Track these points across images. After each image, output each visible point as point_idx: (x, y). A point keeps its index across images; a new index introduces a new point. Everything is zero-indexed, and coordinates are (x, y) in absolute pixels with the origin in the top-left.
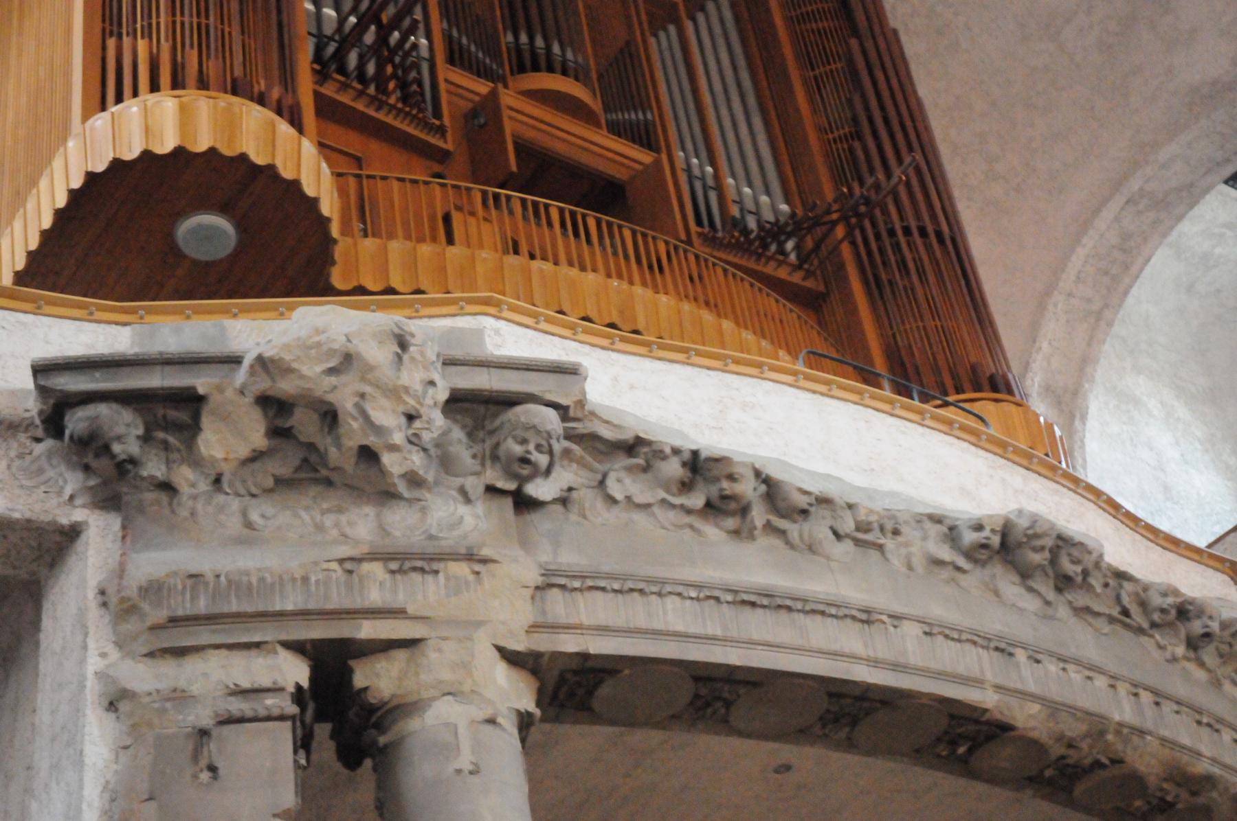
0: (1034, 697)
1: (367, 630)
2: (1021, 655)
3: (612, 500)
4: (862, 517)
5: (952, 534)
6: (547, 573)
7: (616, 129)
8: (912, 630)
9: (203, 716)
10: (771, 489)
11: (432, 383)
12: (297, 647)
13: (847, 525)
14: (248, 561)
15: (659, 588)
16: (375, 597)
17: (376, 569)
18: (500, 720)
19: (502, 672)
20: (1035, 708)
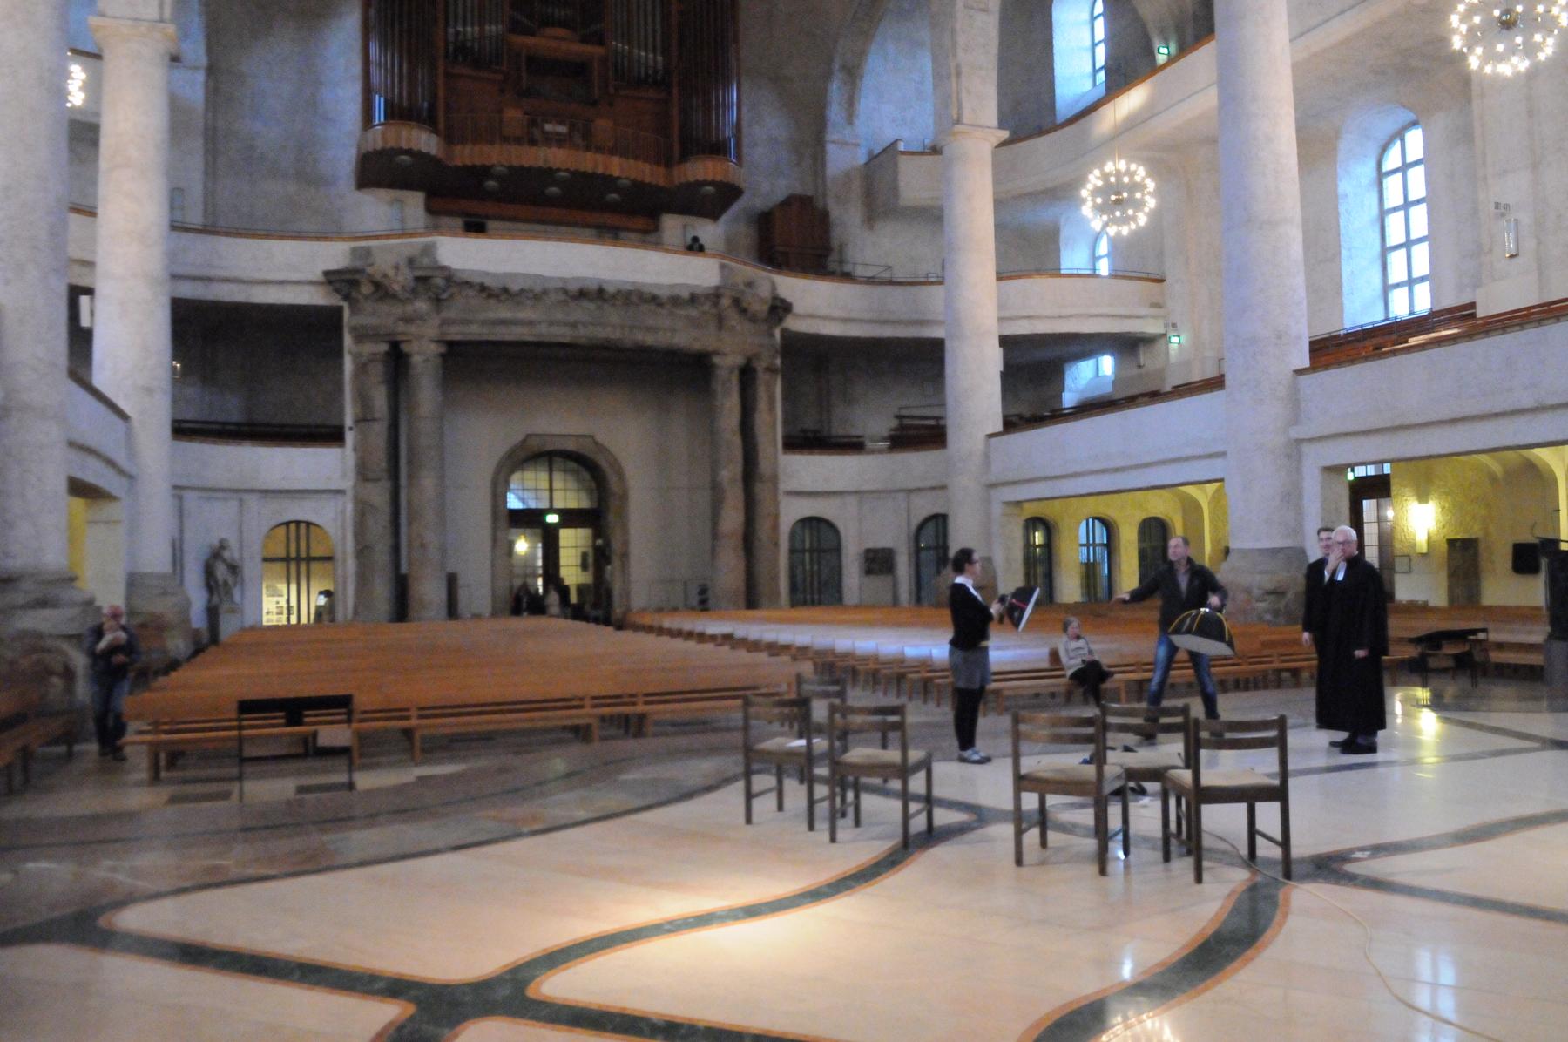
1: (399, 338)
5: (565, 291)
7: (584, 40)
9: (364, 359)
10: (505, 290)
12: (386, 342)
13: (531, 295)
14: (374, 321)
15: (468, 322)
17: (401, 323)
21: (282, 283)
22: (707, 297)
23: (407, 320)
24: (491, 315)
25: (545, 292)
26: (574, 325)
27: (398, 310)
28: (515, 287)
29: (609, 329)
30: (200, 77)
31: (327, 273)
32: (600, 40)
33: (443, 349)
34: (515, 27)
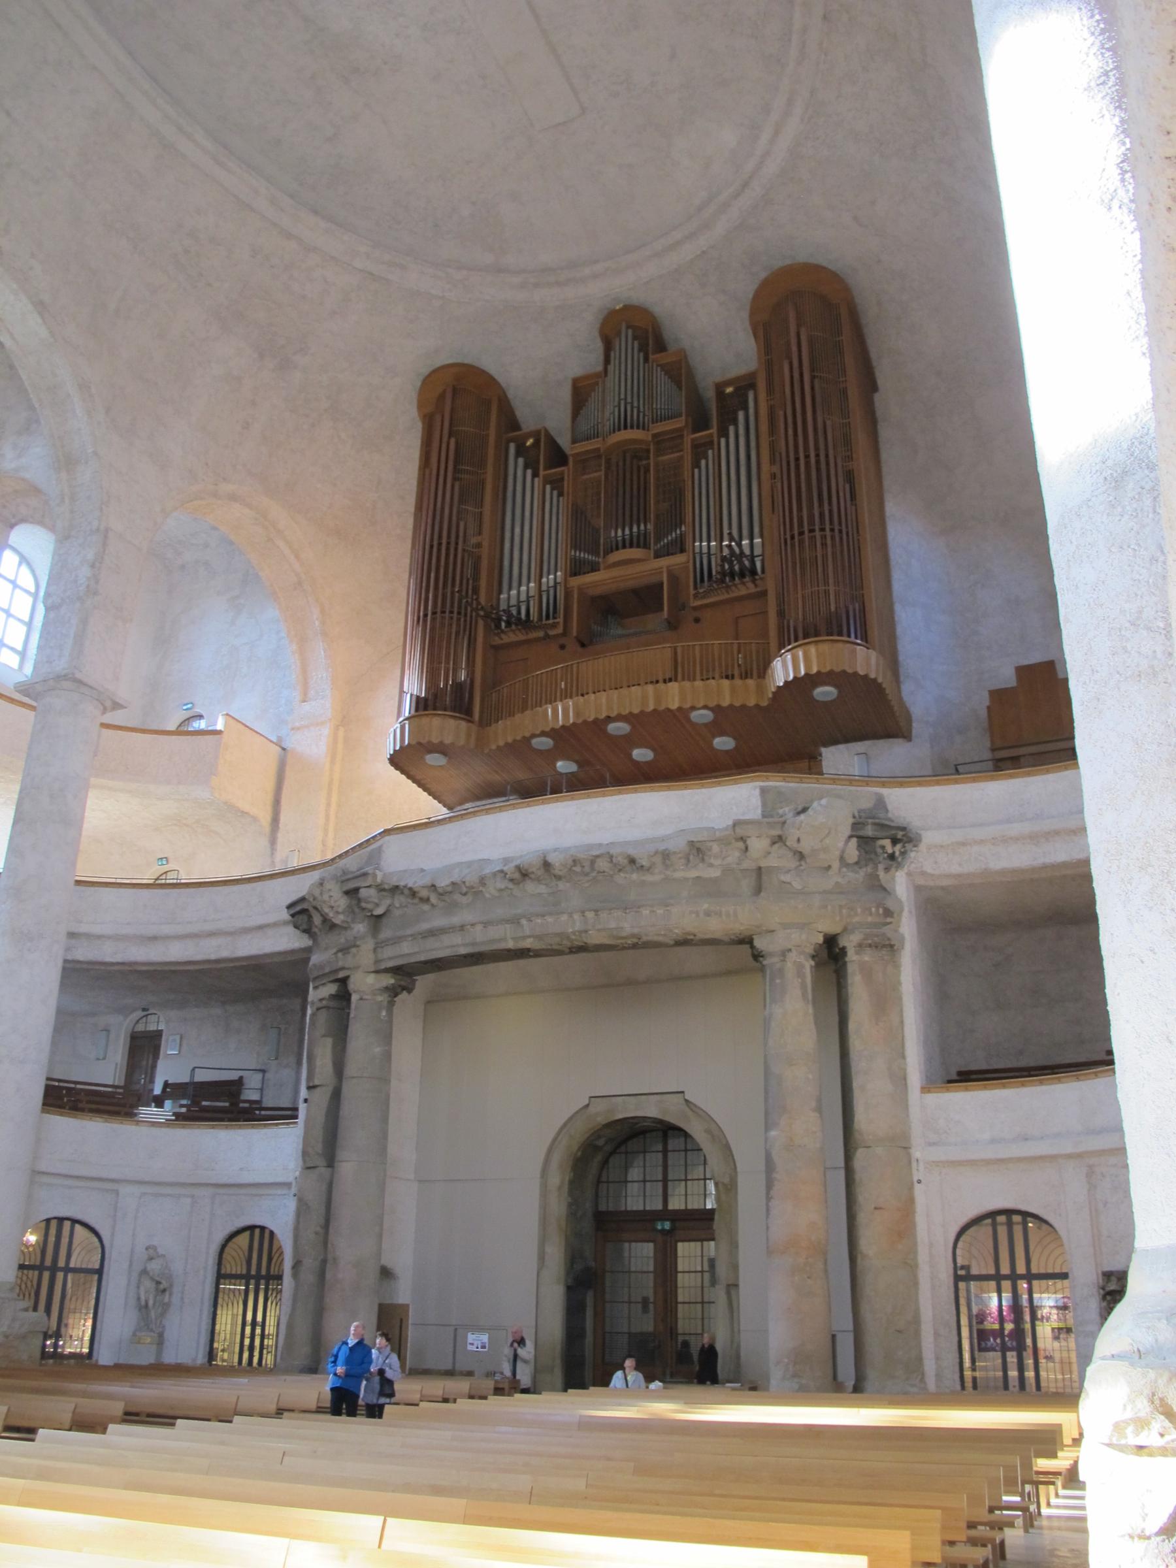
0: (529, 937)
1: (341, 975)
2: (524, 922)
3: (397, 908)
4: (467, 884)
6: (377, 943)
8: (479, 927)
11: (331, 896)
16: (340, 964)
17: (340, 955)
18: (365, 997)
19: (371, 979)
20: (531, 940)
21: (261, 928)
22: (723, 841)
23: (345, 950)
24: (425, 926)
25: (482, 881)
26: (515, 921)
27: (341, 939)
28: (443, 883)
29: (564, 918)
30: (326, 731)
31: (289, 907)
32: (680, 546)
33: (389, 980)
34: (577, 569)
